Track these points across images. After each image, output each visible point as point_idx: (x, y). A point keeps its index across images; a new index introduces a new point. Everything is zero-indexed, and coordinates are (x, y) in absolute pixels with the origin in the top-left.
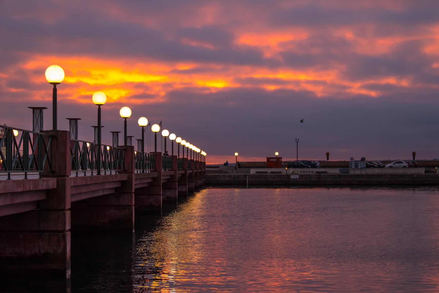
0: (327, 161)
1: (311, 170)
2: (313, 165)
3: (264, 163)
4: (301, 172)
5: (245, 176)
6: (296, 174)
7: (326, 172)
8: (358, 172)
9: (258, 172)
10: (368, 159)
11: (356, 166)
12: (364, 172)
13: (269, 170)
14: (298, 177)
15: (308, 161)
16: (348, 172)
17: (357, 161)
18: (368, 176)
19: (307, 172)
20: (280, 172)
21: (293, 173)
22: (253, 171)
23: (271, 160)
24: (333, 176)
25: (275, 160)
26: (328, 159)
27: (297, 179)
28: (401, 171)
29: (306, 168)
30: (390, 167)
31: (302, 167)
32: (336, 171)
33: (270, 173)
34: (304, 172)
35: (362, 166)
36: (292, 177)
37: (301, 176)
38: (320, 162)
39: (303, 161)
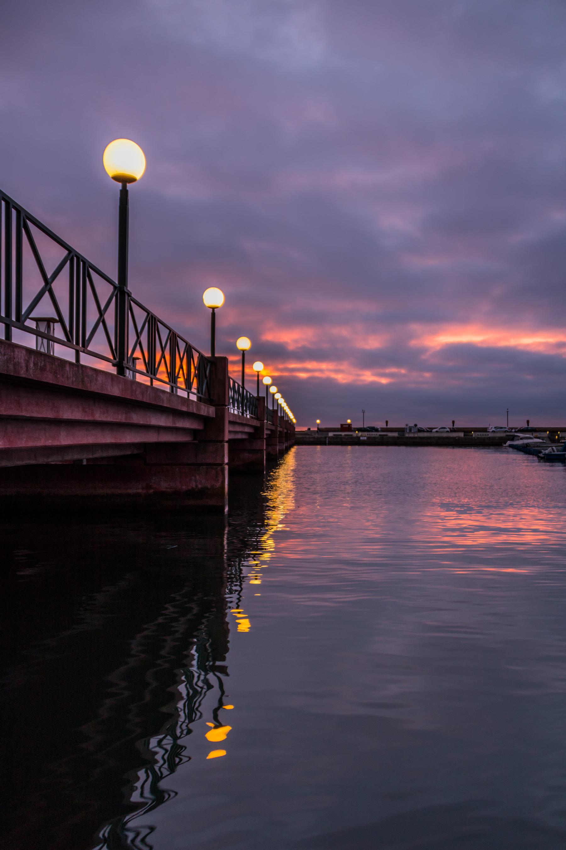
0: (386, 427)
1: (375, 433)
2: (376, 430)
3: (338, 428)
4: (368, 435)
5: (326, 437)
6: (365, 436)
7: (387, 435)
8: (411, 435)
9: (334, 435)
10: (419, 426)
11: (410, 430)
12: (416, 435)
13: (343, 434)
14: (366, 438)
15: (372, 427)
16: (404, 435)
19: (372, 435)
20: (352, 435)
21: (361, 436)
22: (331, 434)
23: (344, 426)
24: (393, 438)
25: (347, 426)
26: (387, 425)
27: (365, 440)
28: (445, 435)
29: (371, 432)
30: (437, 432)
32: (396, 434)
33: (344, 436)
34: (370, 435)
35: (415, 431)
36: (361, 438)
37: (368, 438)
39: (369, 427)
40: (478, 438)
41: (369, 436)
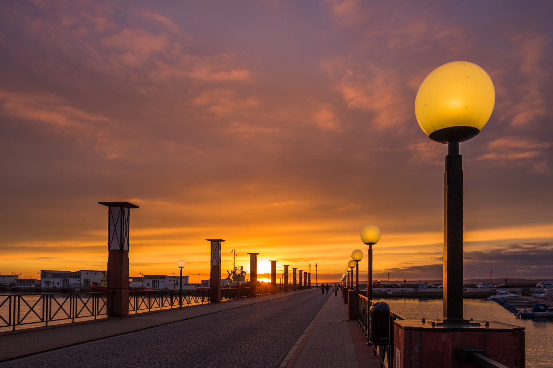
1: (398, 289)
2: (398, 287)
6: (390, 290)
7: (406, 290)
8: (423, 290)
11: (422, 287)
12: (426, 290)
16: (418, 291)
17: (423, 284)
18: (430, 292)
19: (395, 290)
20: (381, 290)
23: (375, 283)
24: (411, 292)
25: (377, 283)
29: (394, 288)
31: (392, 287)
32: (412, 290)
34: (394, 290)
36: (388, 293)
37: (393, 292)
38: (401, 285)
39: (393, 285)
40: (471, 292)
41: (393, 291)
